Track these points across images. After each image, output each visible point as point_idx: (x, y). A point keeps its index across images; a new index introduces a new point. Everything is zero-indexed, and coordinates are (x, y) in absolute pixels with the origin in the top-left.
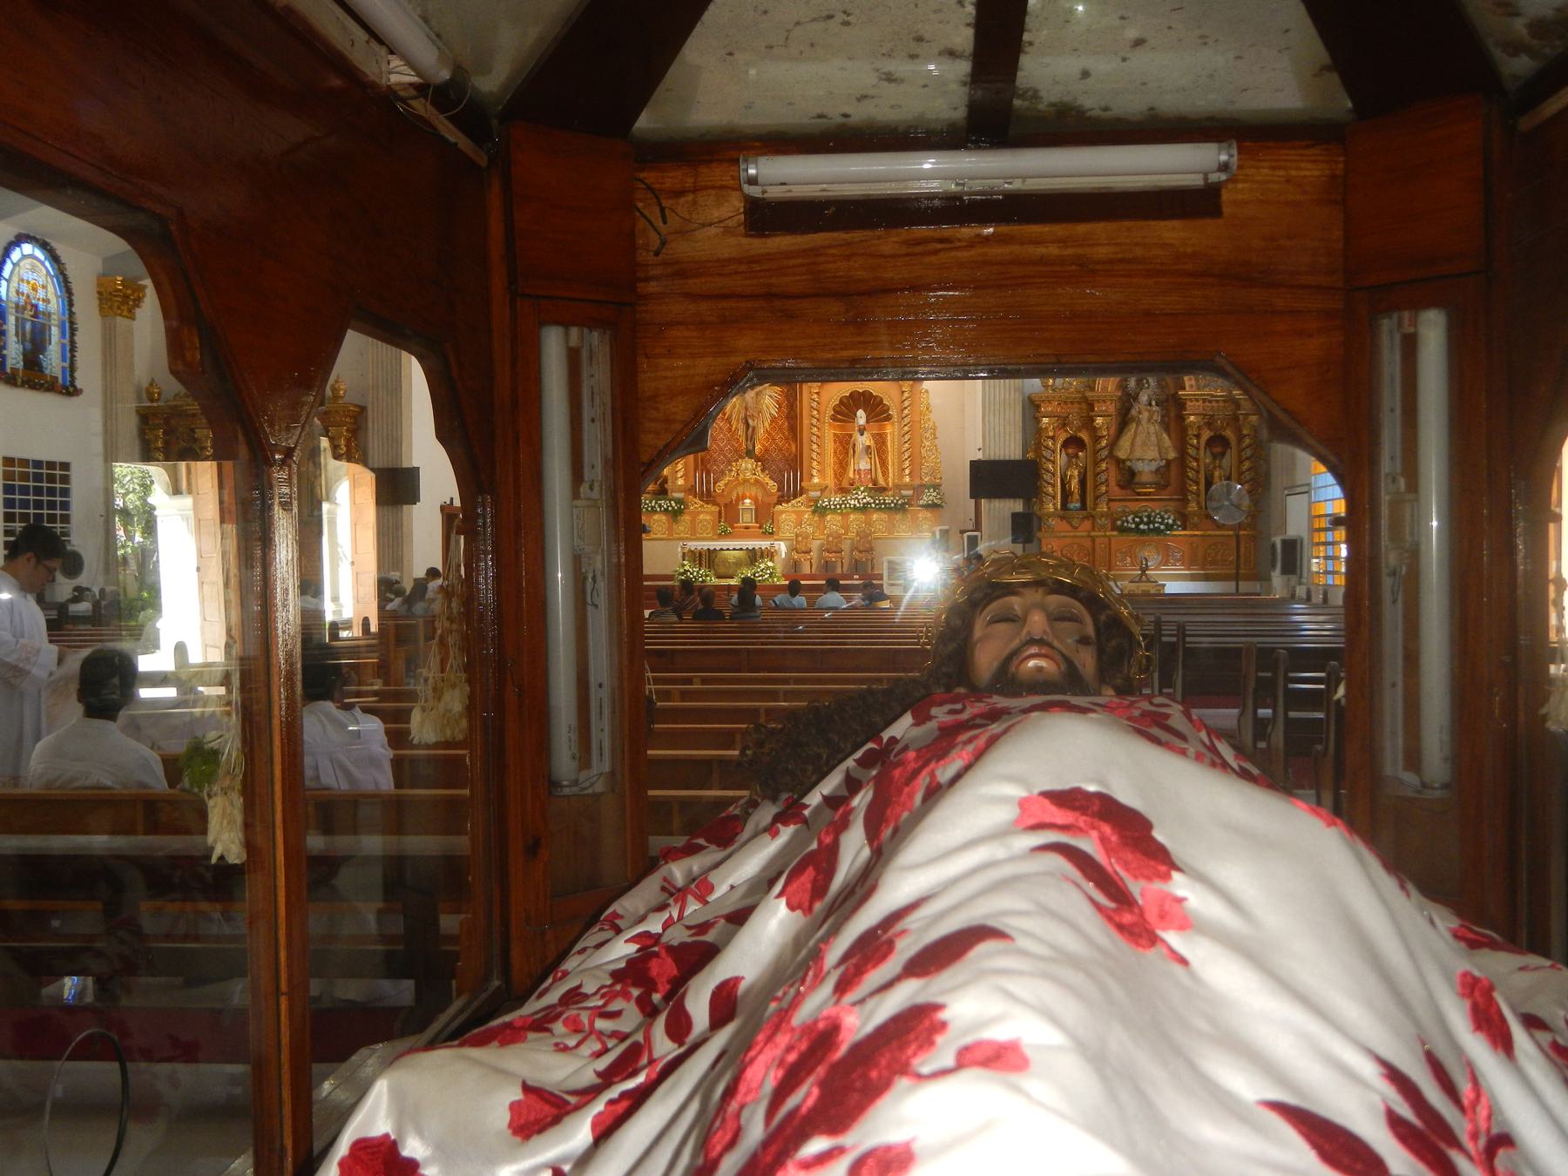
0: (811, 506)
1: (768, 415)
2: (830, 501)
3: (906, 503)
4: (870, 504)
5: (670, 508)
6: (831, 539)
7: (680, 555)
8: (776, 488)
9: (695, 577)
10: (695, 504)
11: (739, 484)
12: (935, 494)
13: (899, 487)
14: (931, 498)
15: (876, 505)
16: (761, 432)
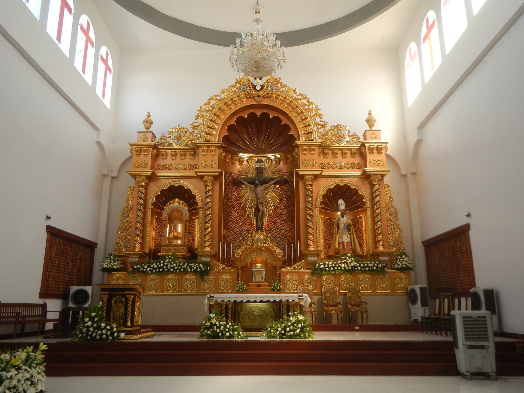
0: (310, 269)
1: (272, 205)
2: (324, 264)
3: (384, 267)
4: (357, 267)
5: (199, 269)
6: (328, 295)
7: (206, 308)
8: (282, 254)
9: (221, 332)
10: (219, 267)
11: (254, 251)
12: (406, 259)
13: (375, 256)
14: (404, 262)
15: (362, 268)
16: (266, 219)
